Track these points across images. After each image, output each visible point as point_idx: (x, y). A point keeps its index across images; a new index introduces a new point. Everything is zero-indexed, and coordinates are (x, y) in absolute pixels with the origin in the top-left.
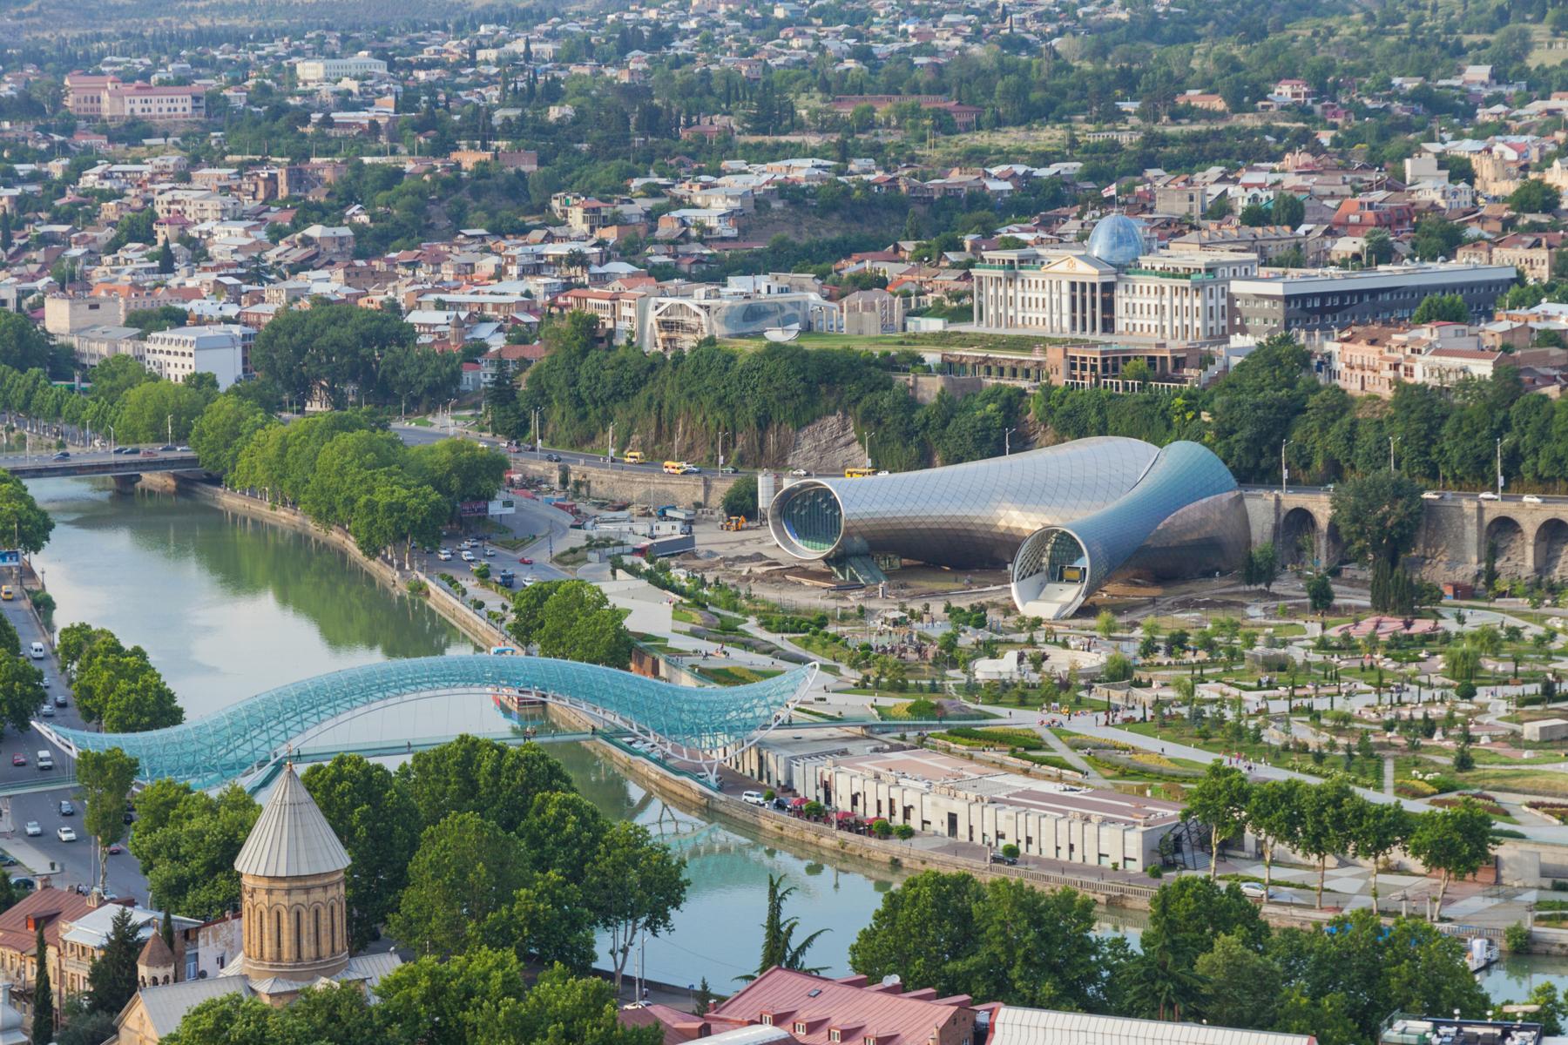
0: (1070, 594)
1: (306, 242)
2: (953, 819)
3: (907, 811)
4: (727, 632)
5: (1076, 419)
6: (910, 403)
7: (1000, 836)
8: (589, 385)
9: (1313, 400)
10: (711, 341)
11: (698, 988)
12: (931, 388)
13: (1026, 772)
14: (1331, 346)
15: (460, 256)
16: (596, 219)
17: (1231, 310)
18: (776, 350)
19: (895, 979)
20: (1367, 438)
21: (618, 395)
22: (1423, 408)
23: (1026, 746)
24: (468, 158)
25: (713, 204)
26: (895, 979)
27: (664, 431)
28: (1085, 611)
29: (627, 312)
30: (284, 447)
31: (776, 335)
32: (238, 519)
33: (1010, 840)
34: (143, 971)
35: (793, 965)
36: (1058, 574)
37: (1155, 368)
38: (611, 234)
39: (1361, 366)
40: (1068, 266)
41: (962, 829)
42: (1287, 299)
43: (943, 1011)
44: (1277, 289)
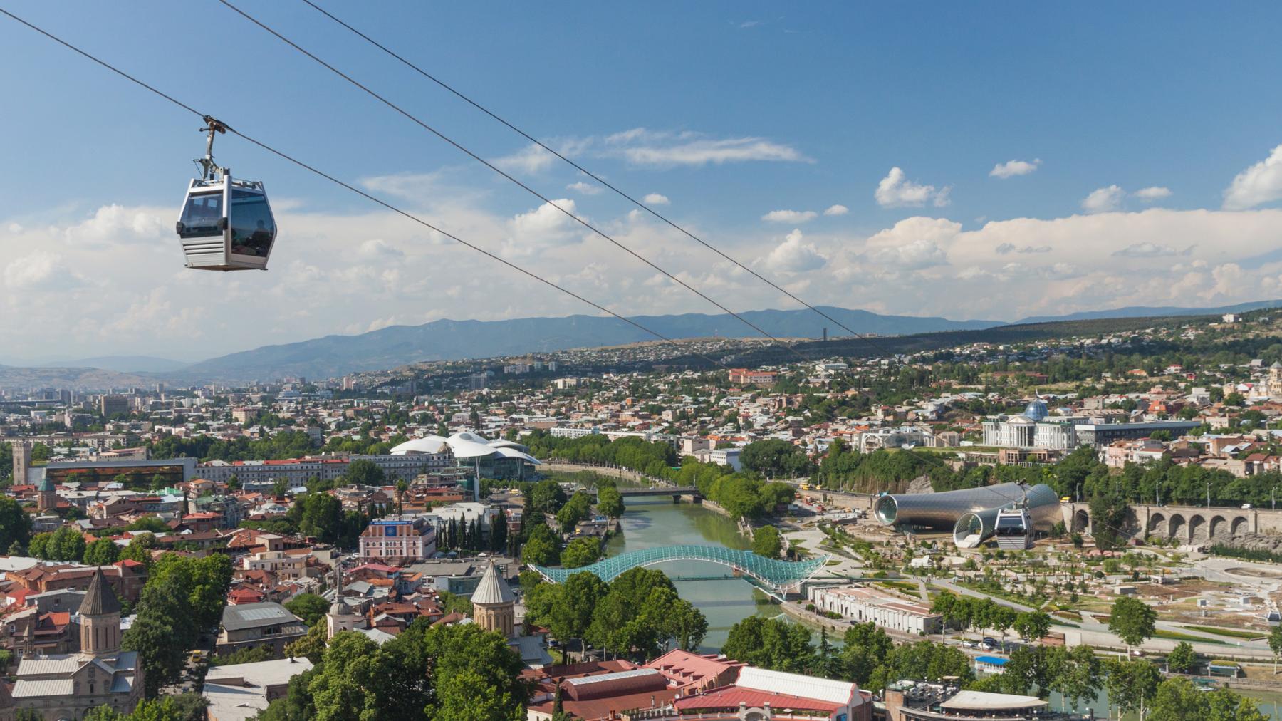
0: (975, 539)
1: (786, 422)
4: (835, 548)
5: (1006, 475)
6: (951, 470)
8: (842, 468)
9: (1094, 469)
10: (882, 449)
12: (957, 466)
14: (1104, 448)
15: (835, 426)
16: (887, 413)
17: (1077, 437)
18: (903, 452)
19: (724, 656)
20: (1115, 484)
21: (850, 470)
22: (1134, 471)
23: (908, 589)
24: (851, 392)
25: (929, 408)
26: (724, 656)
27: (864, 483)
28: (978, 546)
29: (856, 438)
30: (722, 483)
31: (906, 446)
32: (713, 513)
36: (974, 532)
37: (1041, 458)
38: (890, 418)
39: (1113, 456)
40: (1017, 420)
42: (1097, 432)
44: (1092, 428)
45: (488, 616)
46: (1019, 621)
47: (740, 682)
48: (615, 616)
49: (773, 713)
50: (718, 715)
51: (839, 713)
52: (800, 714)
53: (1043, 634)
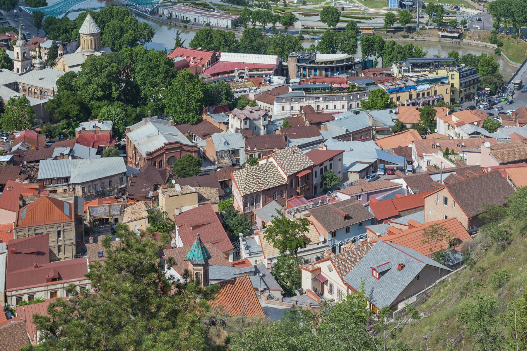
2: (195, 19)
3: (187, 18)
7: (204, 22)
11: (164, 51)
13: (208, 10)
19: (200, 48)
26: (200, 48)
33: (206, 22)
34: (59, 52)
35: (180, 46)
41: (197, 21)
43: (211, 54)
45: (95, 40)
46: (284, 20)
47: (220, 60)
48: (117, 33)
49: (249, 72)
50: (227, 75)
51: (276, 68)
52: (259, 71)
53: (292, 24)
